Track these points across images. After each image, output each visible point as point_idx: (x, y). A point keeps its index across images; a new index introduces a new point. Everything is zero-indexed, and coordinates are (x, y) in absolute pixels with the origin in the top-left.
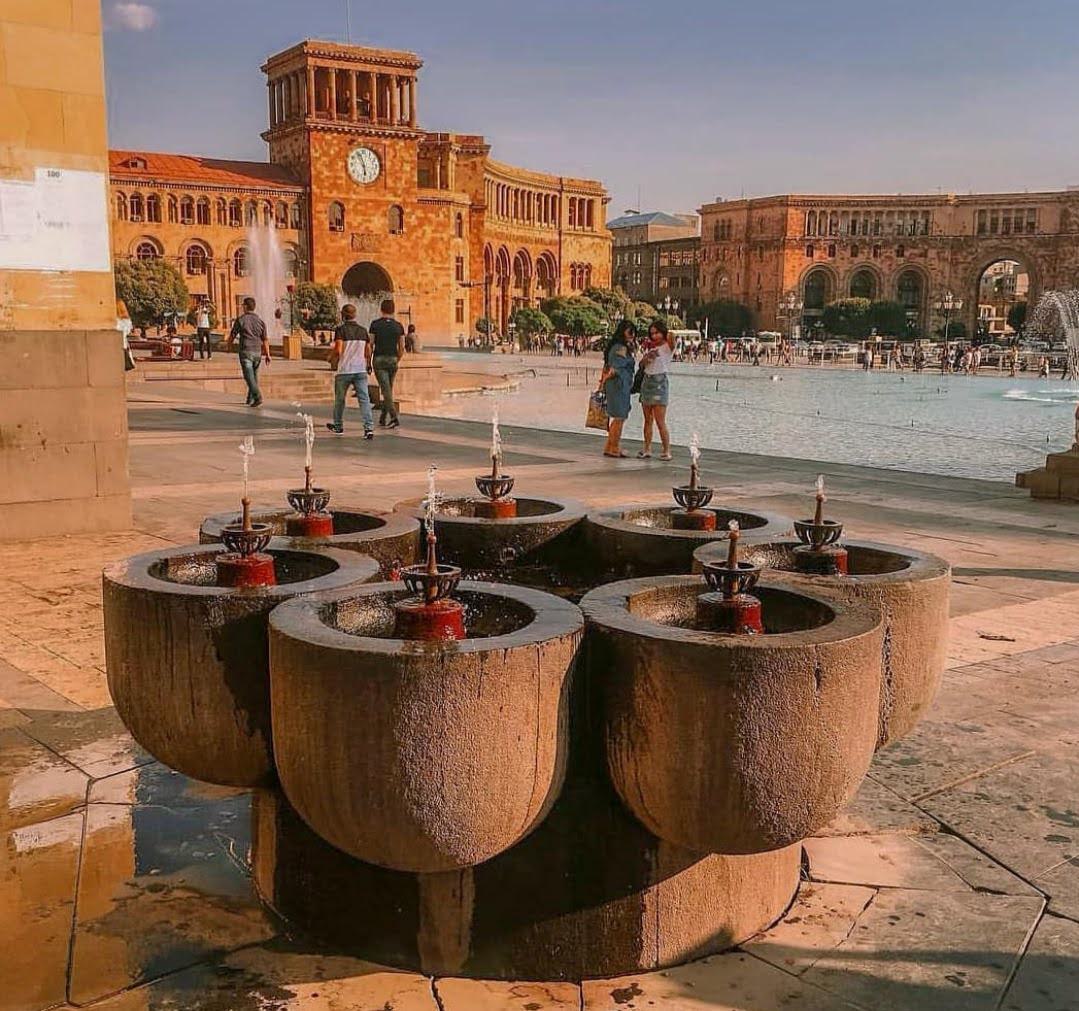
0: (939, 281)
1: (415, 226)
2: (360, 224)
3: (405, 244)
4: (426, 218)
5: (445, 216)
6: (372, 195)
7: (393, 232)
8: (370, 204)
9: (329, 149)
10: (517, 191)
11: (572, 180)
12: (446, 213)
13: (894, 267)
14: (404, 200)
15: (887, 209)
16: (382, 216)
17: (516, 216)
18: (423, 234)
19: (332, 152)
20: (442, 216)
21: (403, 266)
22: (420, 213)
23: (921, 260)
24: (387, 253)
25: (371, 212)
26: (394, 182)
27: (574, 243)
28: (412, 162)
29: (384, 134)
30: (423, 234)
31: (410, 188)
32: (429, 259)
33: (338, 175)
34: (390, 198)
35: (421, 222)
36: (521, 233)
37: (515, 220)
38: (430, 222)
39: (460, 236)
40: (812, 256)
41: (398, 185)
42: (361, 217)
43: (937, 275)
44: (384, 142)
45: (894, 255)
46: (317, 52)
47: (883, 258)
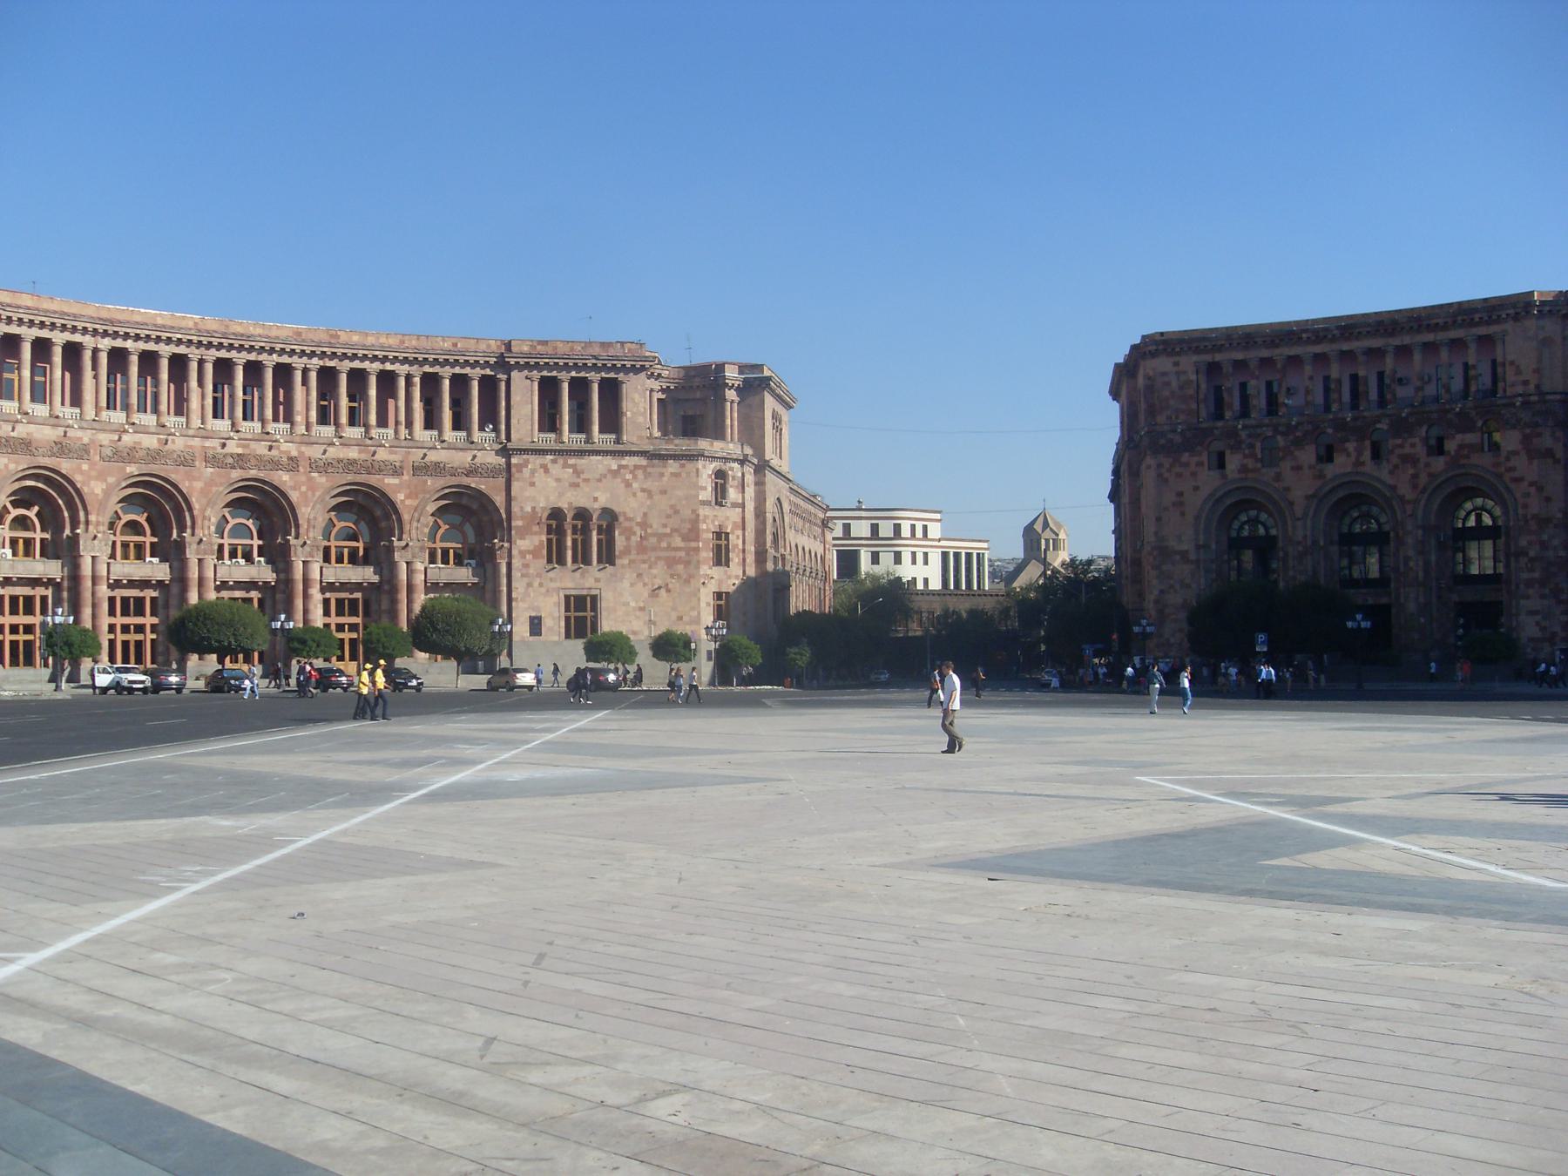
0: (1535, 507)
11: (544, 343)
13: (1423, 479)
15: (1396, 341)
23: (1484, 460)
36: (353, 453)
40: (1221, 465)
45: (1420, 450)
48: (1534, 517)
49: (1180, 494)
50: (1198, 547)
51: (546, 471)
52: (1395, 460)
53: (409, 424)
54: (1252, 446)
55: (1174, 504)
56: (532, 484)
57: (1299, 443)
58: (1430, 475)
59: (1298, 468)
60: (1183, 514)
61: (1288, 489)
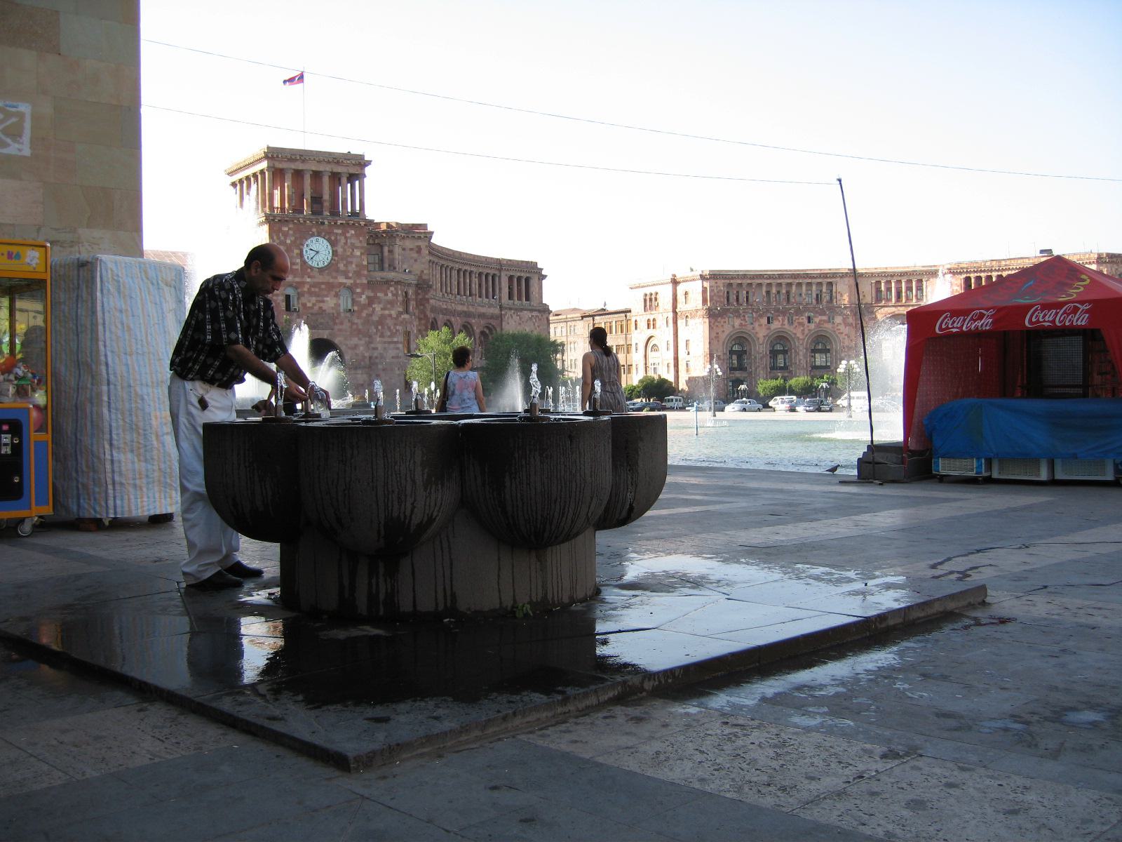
0: (846, 343)
1: (364, 305)
2: (314, 305)
3: (356, 321)
4: (376, 297)
5: (393, 295)
6: (327, 278)
8: (323, 286)
10: (459, 271)
12: (394, 292)
13: (806, 332)
14: (355, 281)
16: (334, 296)
17: (458, 294)
19: (288, 242)
20: (390, 295)
21: (355, 341)
23: (829, 326)
24: (340, 330)
27: (514, 316)
28: (362, 248)
32: (379, 334)
34: (342, 280)
35: (371, 301)
37: (458, 297)
39: (407, 312)
41: (350, 268)
43: (844, 339)
44: (336, 231)
45: (805, 321)
46: (275, 156)
47: (796, 324)
48: (848, 347)
49: (717, 333)
50: (724, 354)
51: (512, 317)
52: (796, 324)
53: (476, 295)
54: (744, 316)
55: (715, 337)
56: (508, 323)
57: (761, 316)
58: (809, 330)
59: (761, 325)
60: (718, 341)
61: (756, 333)
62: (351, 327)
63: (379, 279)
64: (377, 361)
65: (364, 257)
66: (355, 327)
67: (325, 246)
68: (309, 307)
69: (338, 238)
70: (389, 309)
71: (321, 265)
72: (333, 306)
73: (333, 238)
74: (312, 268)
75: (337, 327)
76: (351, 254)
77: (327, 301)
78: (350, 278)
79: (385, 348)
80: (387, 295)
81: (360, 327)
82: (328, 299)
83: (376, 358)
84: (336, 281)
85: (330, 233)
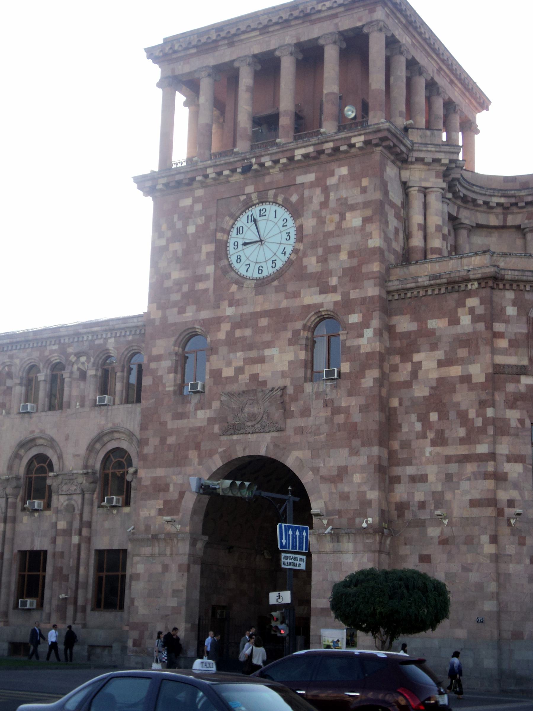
2: (239, 370)
5: (476, 319)
7: (312, 376)
8: (264, 322)
9: (186, 225)
12: (480, 310)
14: (345, 295)
16: (291, 342)
18: (414, 374)
20: (466, 320)
21: (340, 457)
22: (404, 324)
24: (300, 431)
25: (267, 337)
26: (323, 260)
28: (366, 205)
29: (291, 159)
30: (414, 374)
31: (360, 266)
32: (431, 435)
33: (199, 272)
34: (311, 297)
38: (433, 341)
41: (333, 265)
42: (239, 354)
62: (329, 420)
63: (423, 281)
64: (424, 515)
65: (373, 228)
66: (340, 419)
67: (281, 223)
68: (227, 378)
69: (307, 193)
70: (462, 362)
71: (268, 271)
72: (286, 368)
73: (294, 198)
74: (240, 281)
75: (291, 424)
76: (339, 226)
77: (272, 357)
78: (334, 289)
79: (449, 477)
80: (454, 321)
81: (357, 417)
82: (272, 352)
83: (422, 505)
84: (297, 303)
85: (288, 187)
